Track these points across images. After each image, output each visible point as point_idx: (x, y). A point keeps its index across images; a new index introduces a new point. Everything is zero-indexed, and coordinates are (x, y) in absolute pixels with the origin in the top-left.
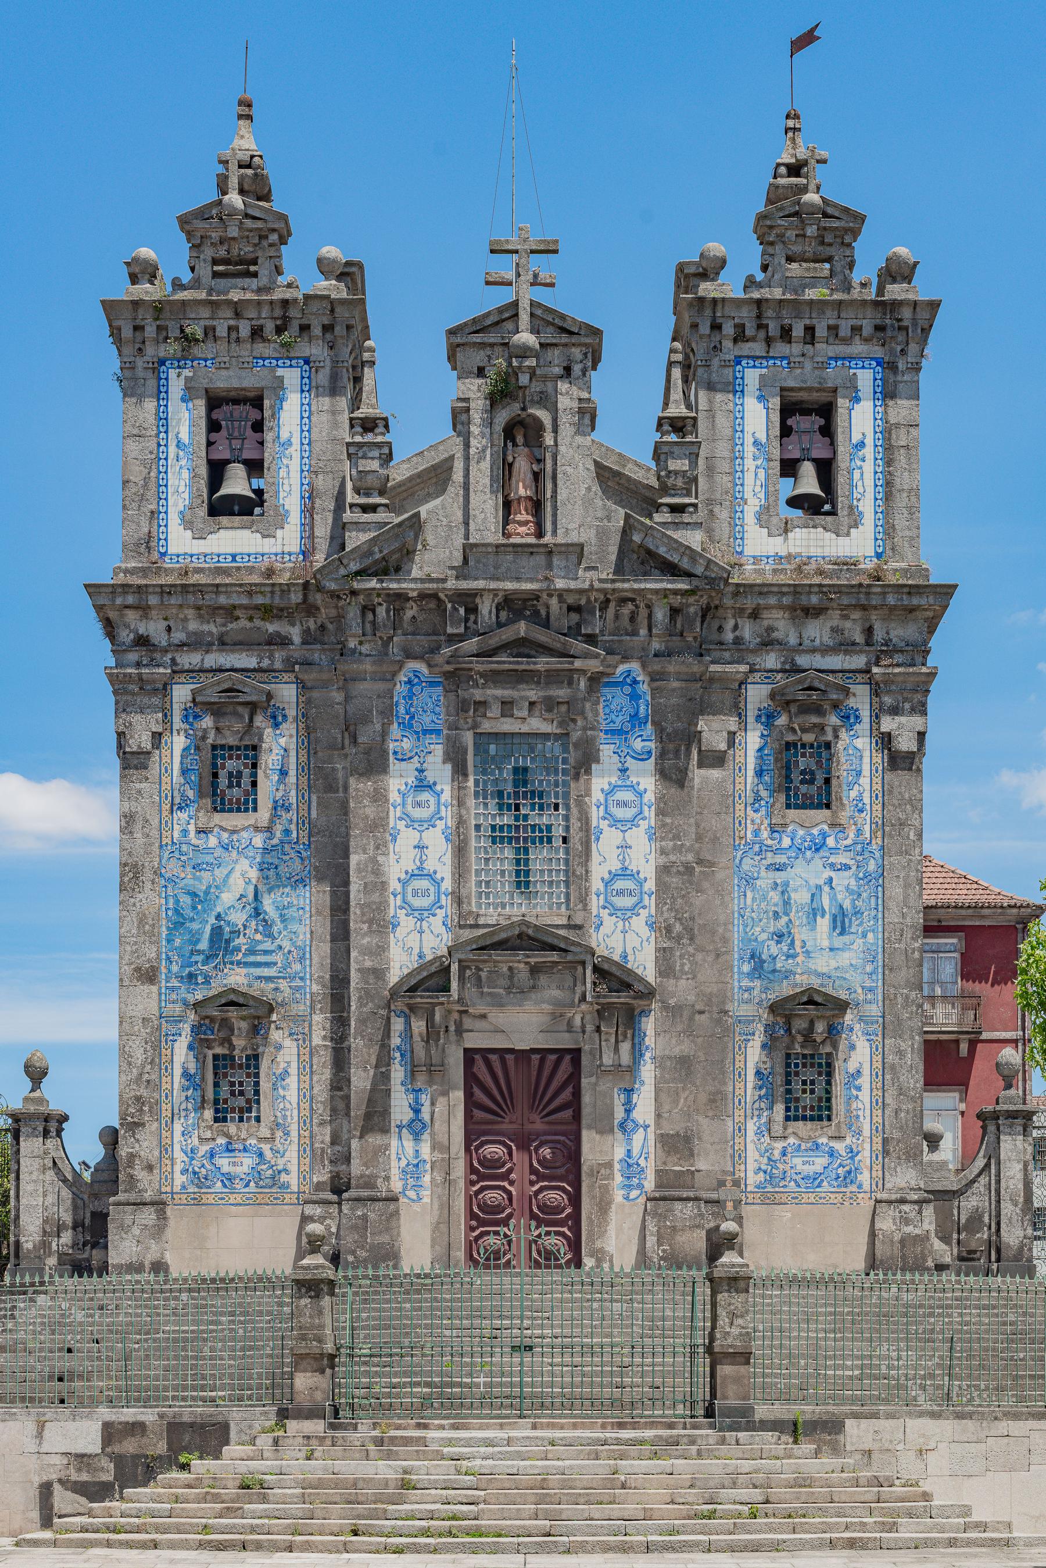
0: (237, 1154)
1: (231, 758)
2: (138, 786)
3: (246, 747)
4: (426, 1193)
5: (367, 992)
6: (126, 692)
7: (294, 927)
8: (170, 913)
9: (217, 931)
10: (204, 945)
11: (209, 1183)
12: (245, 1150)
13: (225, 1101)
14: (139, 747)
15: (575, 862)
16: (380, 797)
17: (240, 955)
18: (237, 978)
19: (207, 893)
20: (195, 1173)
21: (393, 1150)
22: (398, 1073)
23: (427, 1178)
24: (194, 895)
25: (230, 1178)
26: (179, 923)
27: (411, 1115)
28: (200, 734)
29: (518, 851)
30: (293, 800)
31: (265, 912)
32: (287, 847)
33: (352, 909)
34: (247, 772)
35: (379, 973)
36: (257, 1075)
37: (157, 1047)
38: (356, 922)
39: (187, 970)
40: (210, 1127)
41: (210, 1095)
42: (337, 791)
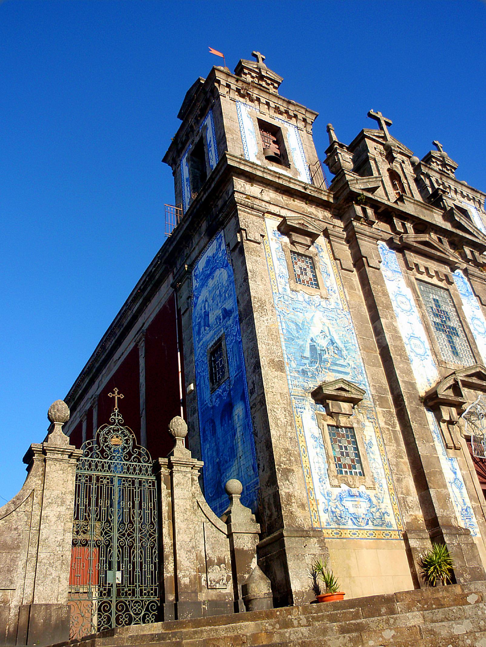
0: (357, 499)
1: (299, 260)
2: (255, 258)
3: (306, 256)
4: (477, 530)
5: (411, 395)
6: (245, 212)
7: (353, 355)
8: (285, 331)
9: (313, 348)
10: (307, 354)
11: (344, 521)
12: (360, 496)
13: (339, 459)
14: (255, 239)
15: (473, 346)
16: (385, 294)
17: (329, 365)
18: (330, 377)
19: (303, 324)
20: (333, 512)
21: (452, 499)
22: (440, 447)
23: (474, 520)
24: (297, 325)
25: (356, 518)
26: (290, 339)
27: (453, 475)
28: (283, 244)
29: (447, 335)
30: (336, 289)
31: (336, 343)
32: (339, 311)
33: (389, 347)
34: (308, 270)
35: (412, 385)
36: (355, 443)
37: (291, 414)
38: (393, 355)
39: (301, 368)
40: (337, 477)
41: (331, 453)
42: (355, 290)
